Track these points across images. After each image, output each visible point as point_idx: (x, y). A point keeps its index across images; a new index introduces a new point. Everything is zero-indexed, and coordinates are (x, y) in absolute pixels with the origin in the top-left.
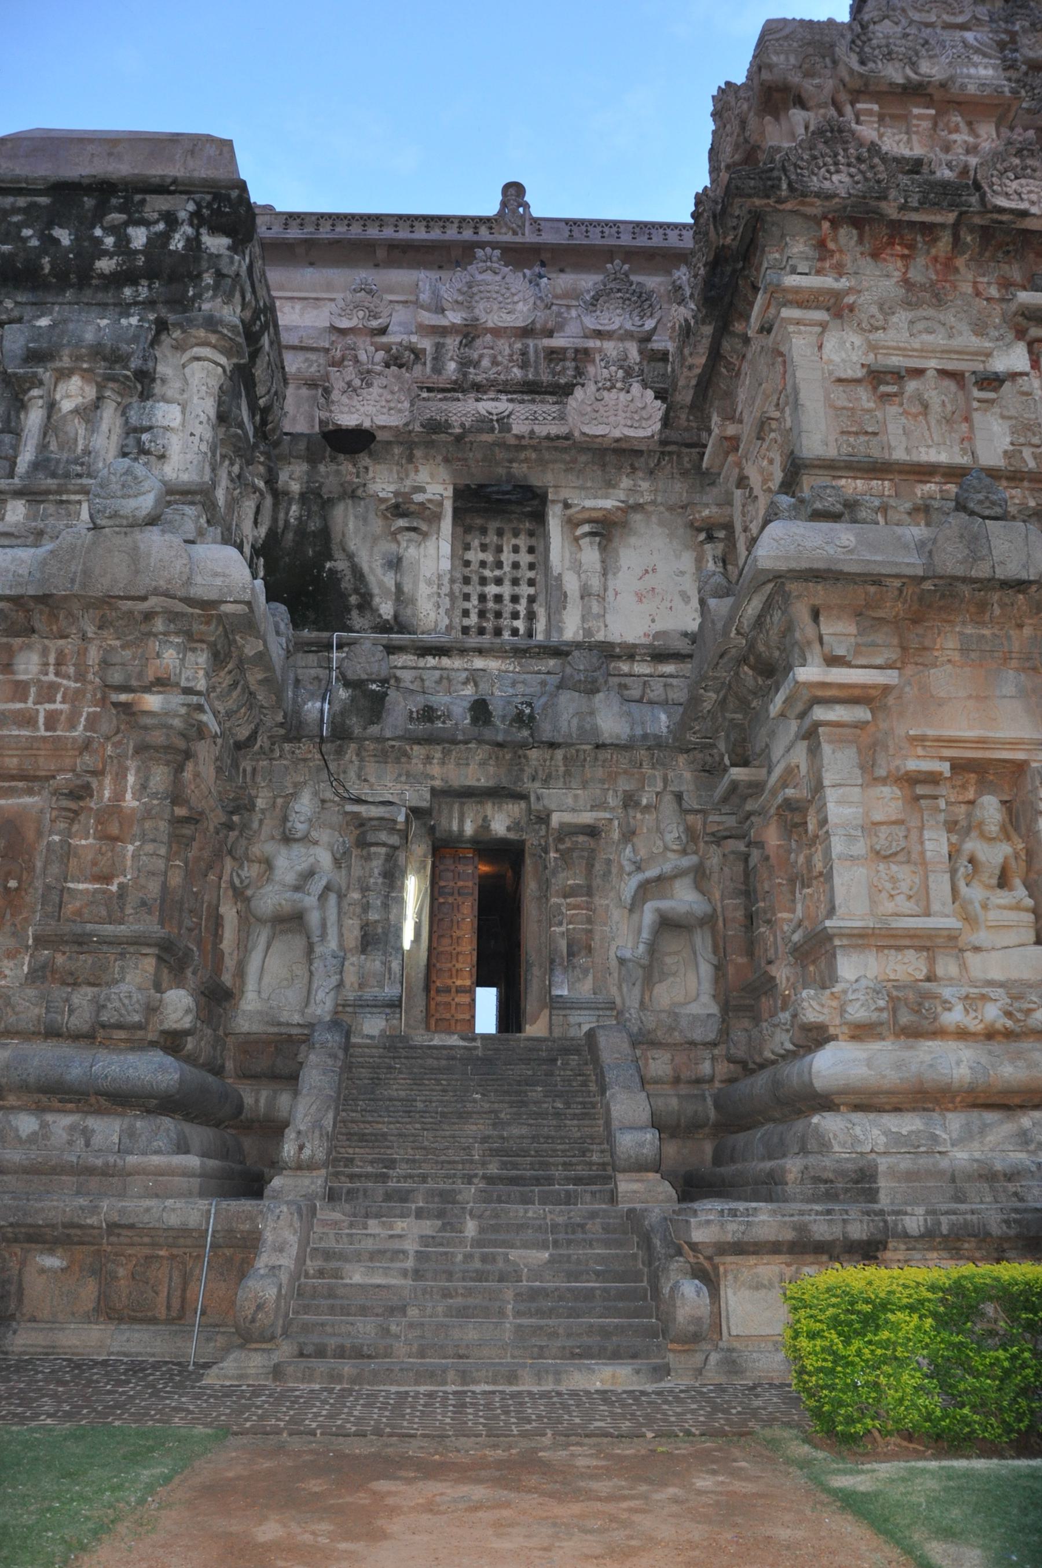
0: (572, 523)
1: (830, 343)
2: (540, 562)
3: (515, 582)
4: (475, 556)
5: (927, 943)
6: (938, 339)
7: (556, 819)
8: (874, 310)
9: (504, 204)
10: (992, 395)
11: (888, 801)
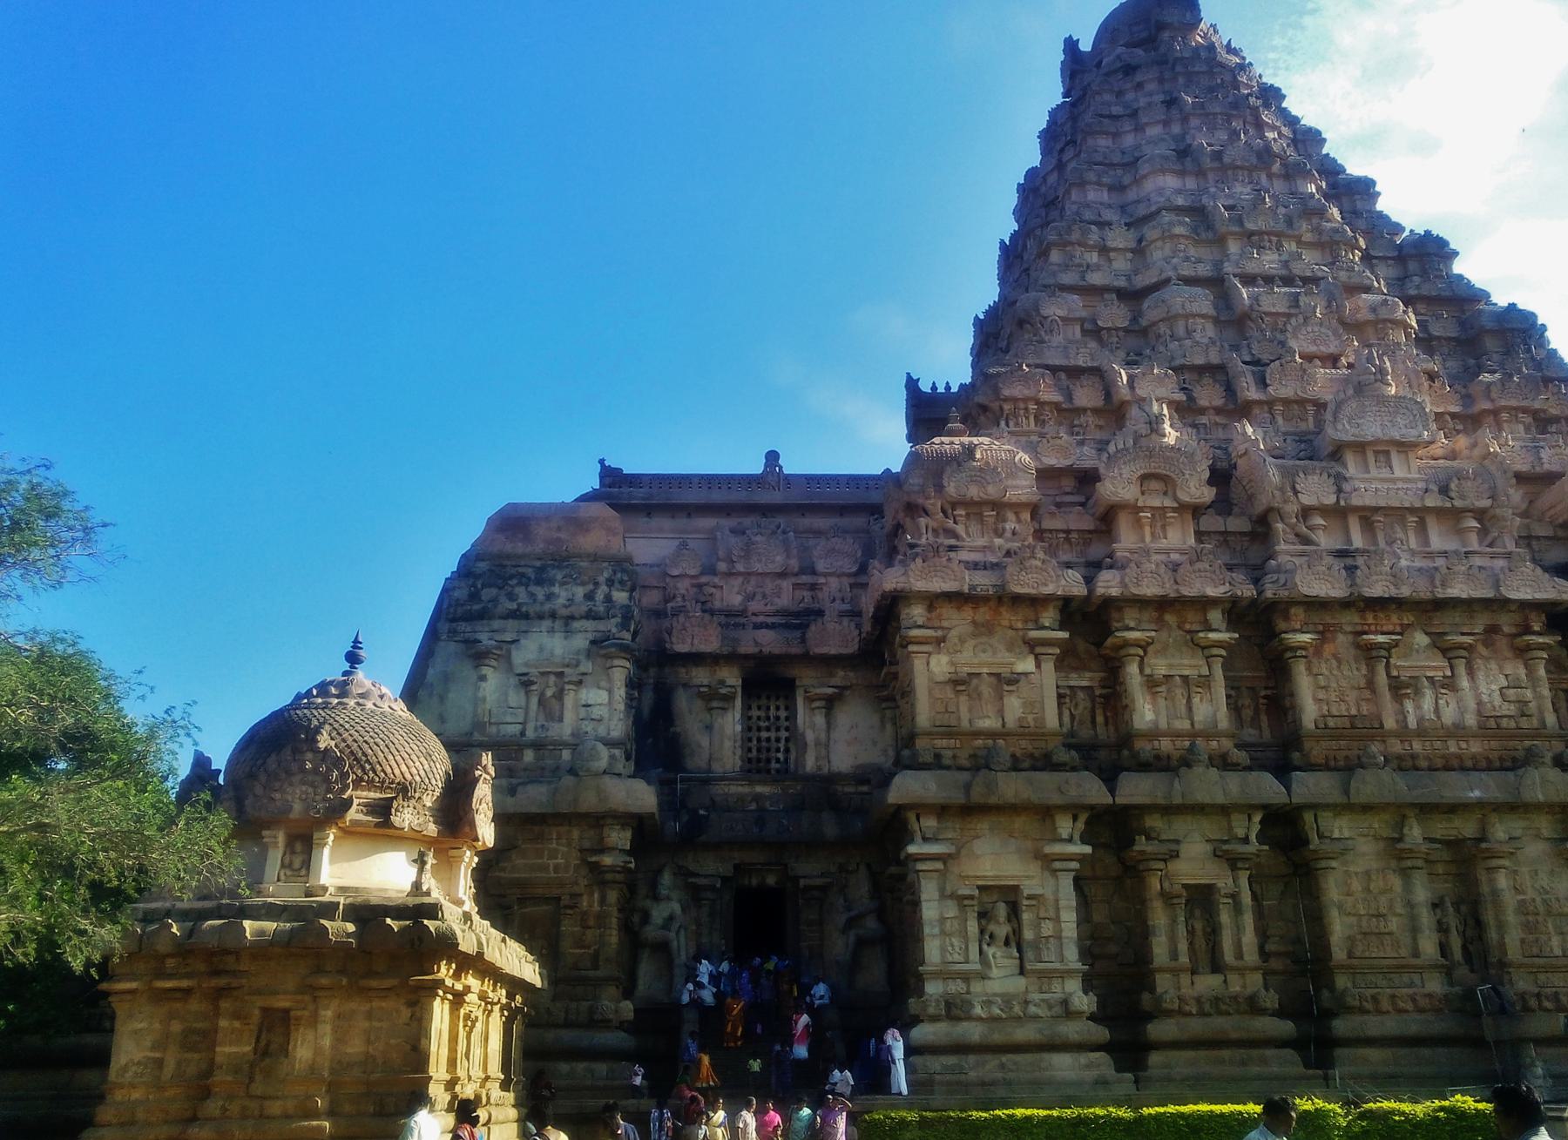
0: (810, 700)
1: (934, 660)
2: (792, 717)
3: (778, 729)
4: (755, 713)
5: (966, 977)
6: (985, 657)
7: (802, 882)
9: (766, 466)
11: (952, 911)
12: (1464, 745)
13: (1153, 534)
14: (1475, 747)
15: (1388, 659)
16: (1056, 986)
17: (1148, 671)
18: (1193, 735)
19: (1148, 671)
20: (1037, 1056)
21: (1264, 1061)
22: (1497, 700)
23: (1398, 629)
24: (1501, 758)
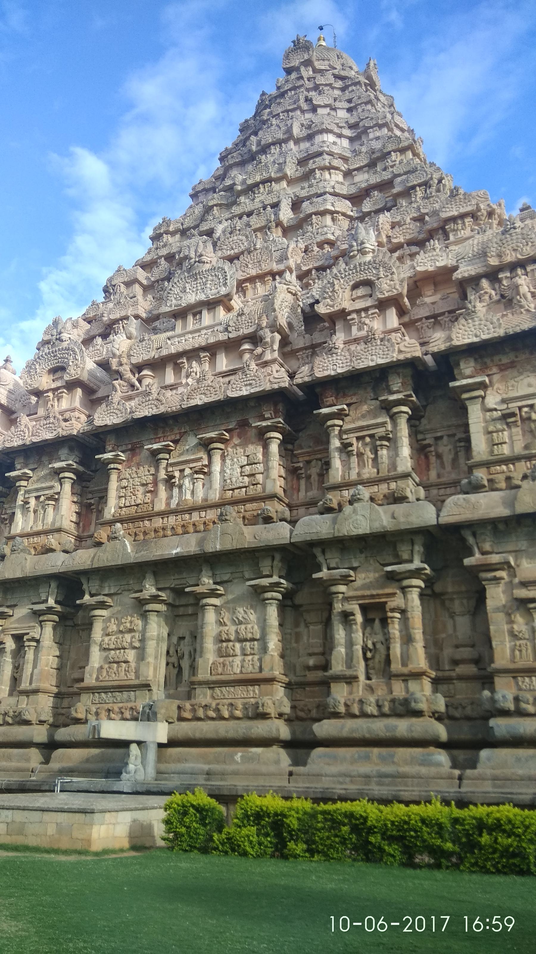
12: (203, 514)
23: (178, 437)
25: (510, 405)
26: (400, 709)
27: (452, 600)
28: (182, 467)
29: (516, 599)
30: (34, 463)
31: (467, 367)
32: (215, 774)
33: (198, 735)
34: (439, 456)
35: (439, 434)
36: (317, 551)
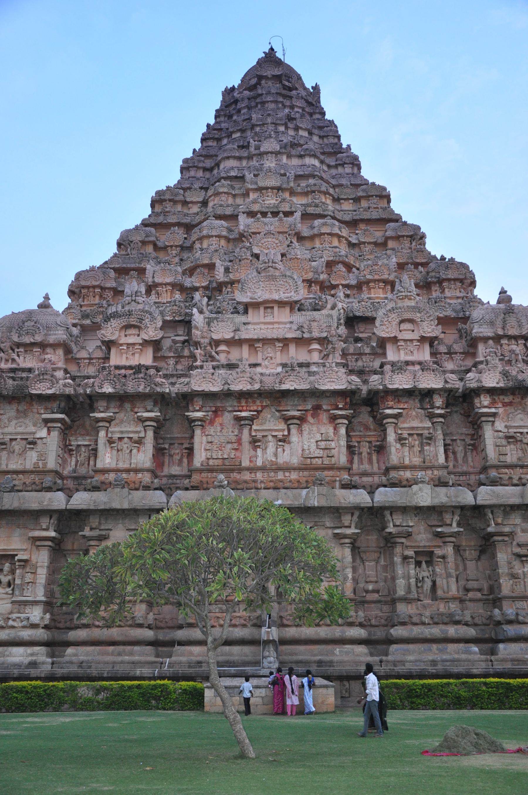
8: (6, 421)
10: (32, 446)
12: (287, 474)
13: (127, 358)
14: (294, 476)
15: (251, 425)
16: (28, 609)
17: (110, 435)
18: (128, 471)
19: (110, 435)
20: (5, 648)
21: (131, 654)
22: (313, 446)
23: (260, 409)
24: (307, 482)
25: (510, 430)
26: (446, 620)
27: (465, 550)
28: (265, 434)
29: (514, 554)
30: (115, 408)
31: (485, 400)
32: (325, 662)
33: (303, 637)
34: (454, 453)
35: (454, 438)
36: (387, 513)
